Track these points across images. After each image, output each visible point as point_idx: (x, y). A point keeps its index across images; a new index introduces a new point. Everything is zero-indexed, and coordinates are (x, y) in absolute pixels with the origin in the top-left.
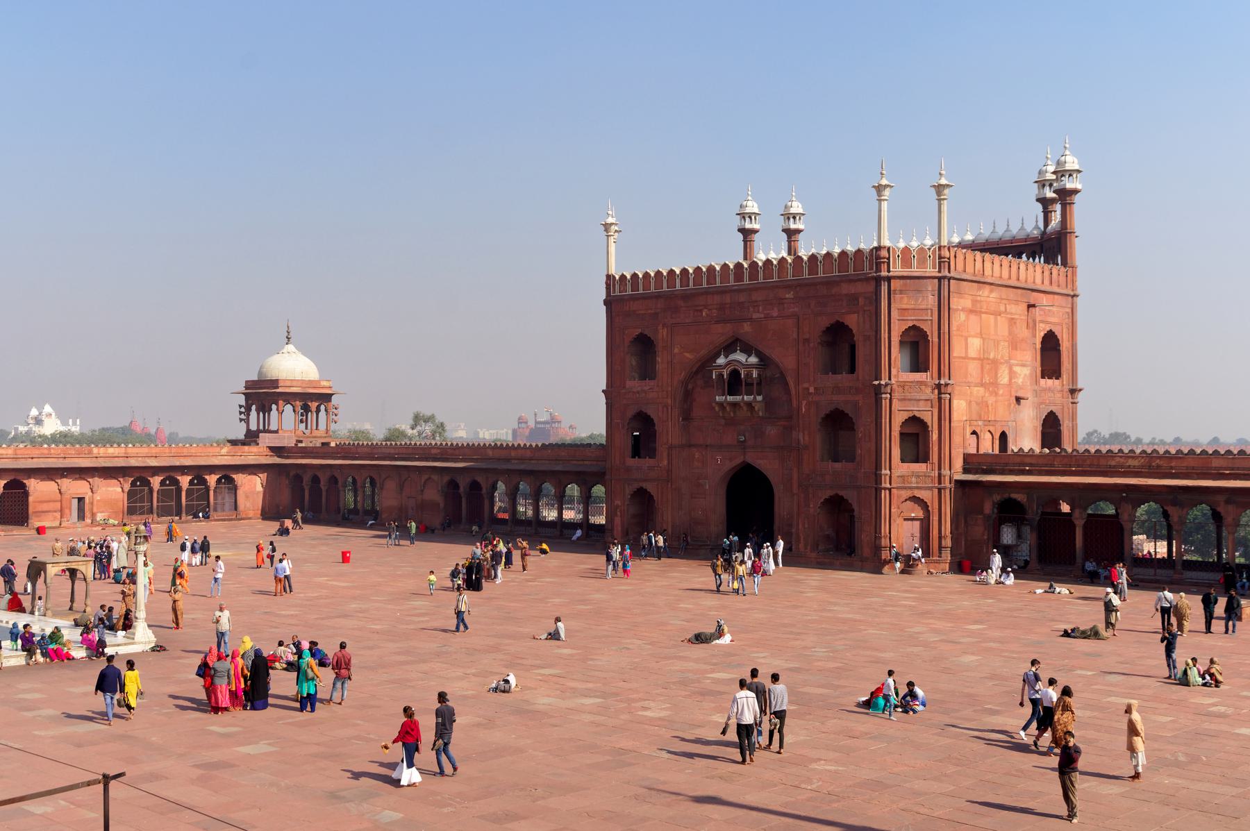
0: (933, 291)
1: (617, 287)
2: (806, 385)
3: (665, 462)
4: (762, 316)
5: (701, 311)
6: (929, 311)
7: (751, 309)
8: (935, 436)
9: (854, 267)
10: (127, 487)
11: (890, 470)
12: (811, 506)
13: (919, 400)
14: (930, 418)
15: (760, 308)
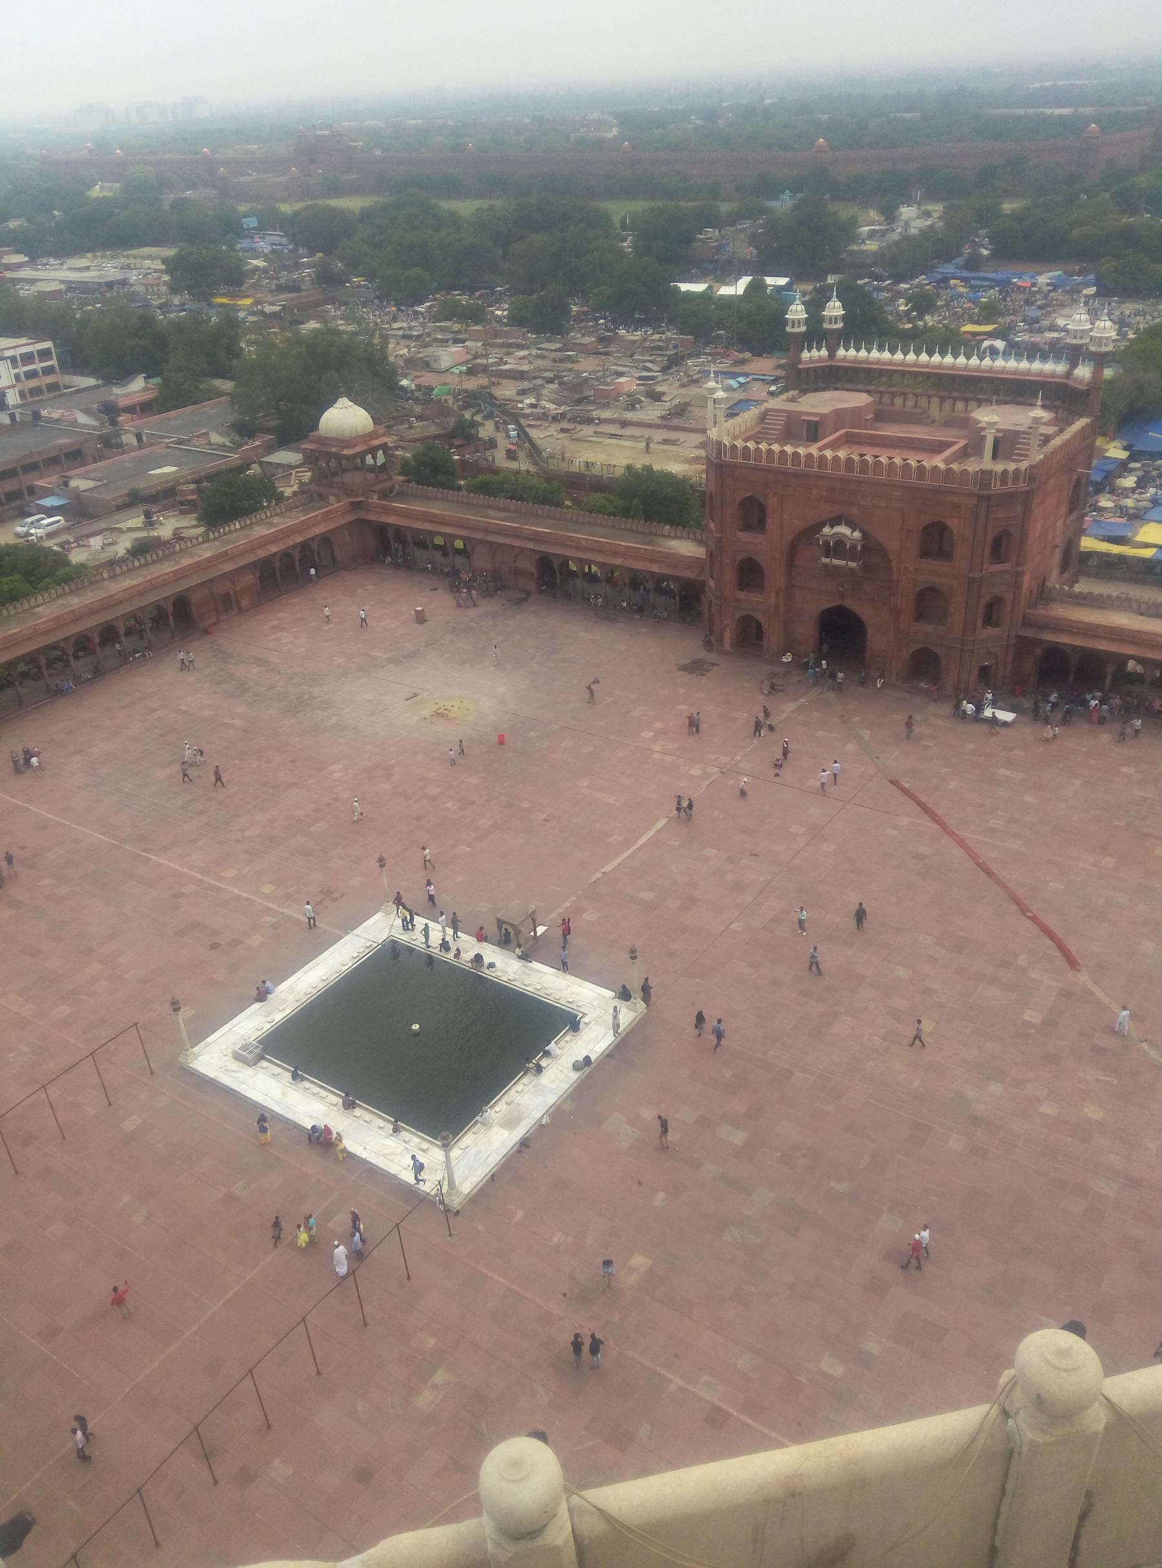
1: (728, 454)
3: (773, 600)
8: (1009, 608)
10: (257, 574)
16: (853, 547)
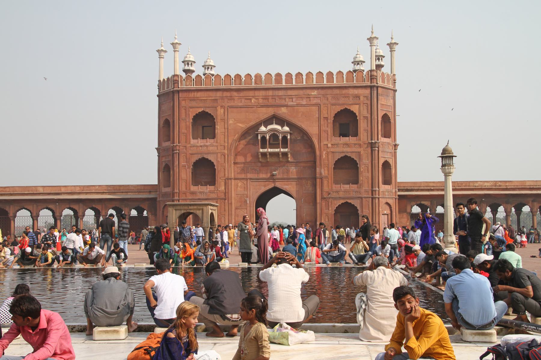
0: (392, 97)
2: (326, 143)
3: (223, 188)
4: (295, 104)
5: (251, 99)
6: (391, 107)
7: (287, 100)
8: (393, 172)
9: (357, 80)
11: (379, 188)
12: (330, 209)
13: (388, 152)
14: (391, 162)
15: (294, 100)
16: (285, 138)
